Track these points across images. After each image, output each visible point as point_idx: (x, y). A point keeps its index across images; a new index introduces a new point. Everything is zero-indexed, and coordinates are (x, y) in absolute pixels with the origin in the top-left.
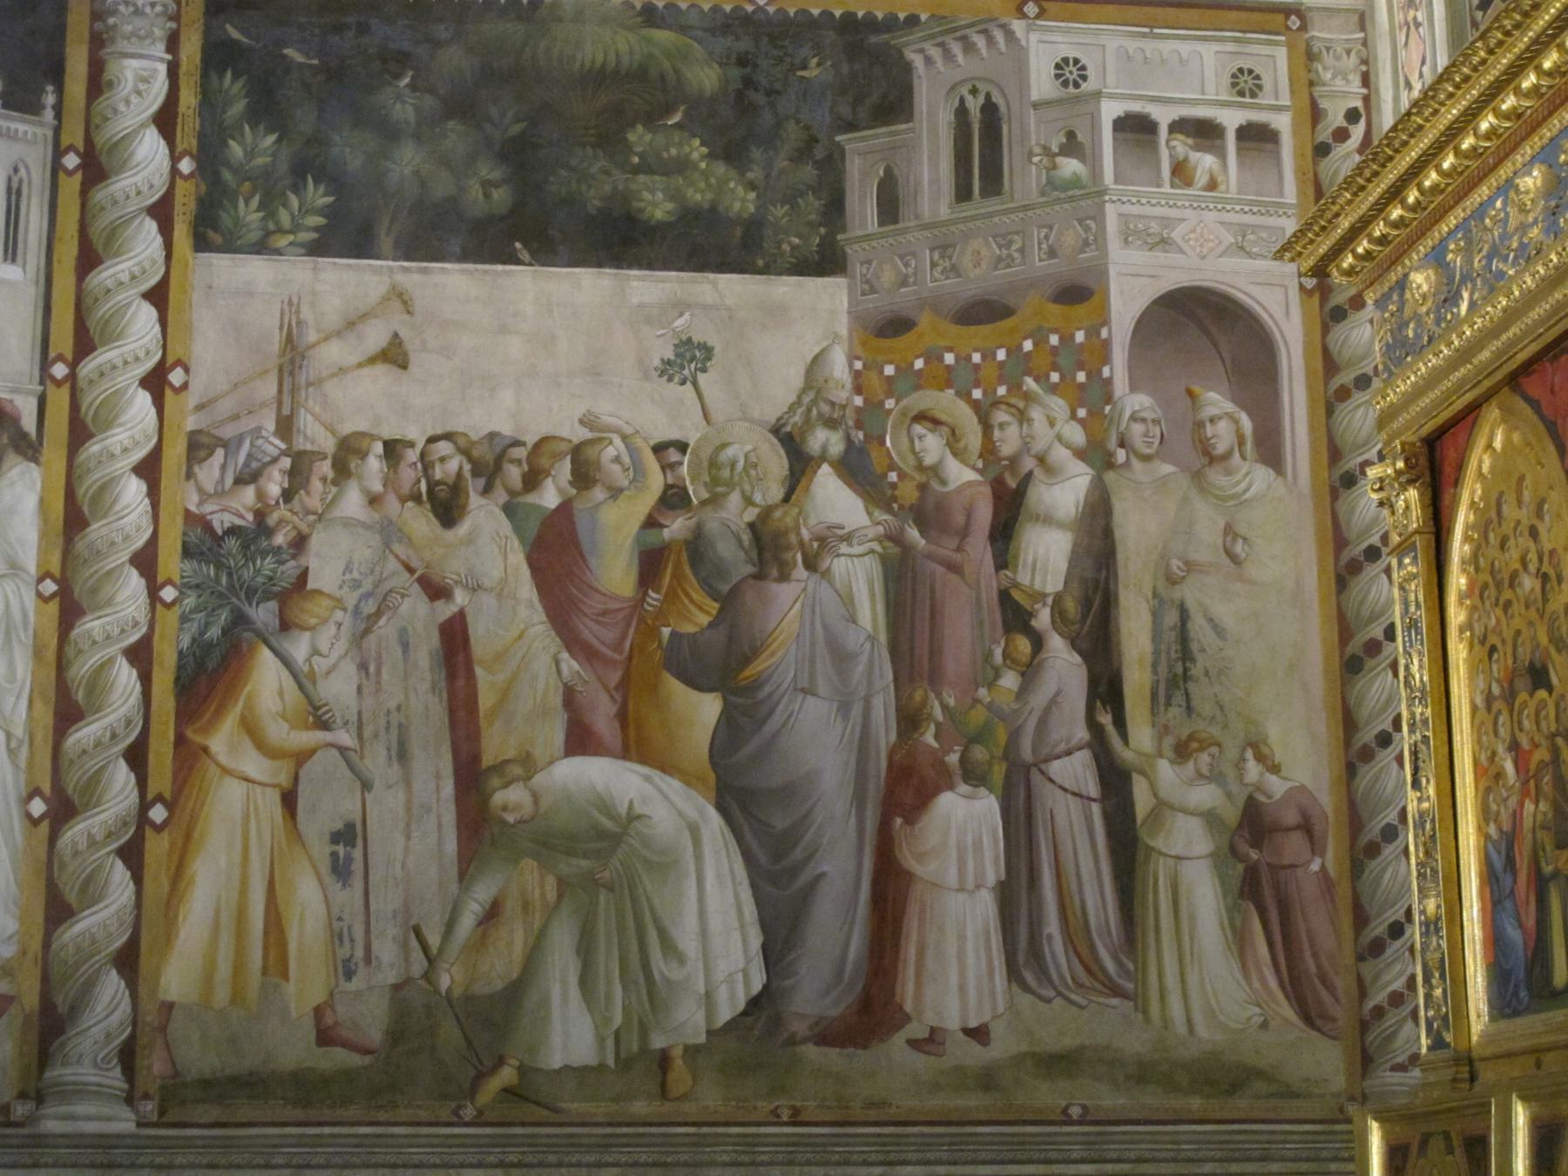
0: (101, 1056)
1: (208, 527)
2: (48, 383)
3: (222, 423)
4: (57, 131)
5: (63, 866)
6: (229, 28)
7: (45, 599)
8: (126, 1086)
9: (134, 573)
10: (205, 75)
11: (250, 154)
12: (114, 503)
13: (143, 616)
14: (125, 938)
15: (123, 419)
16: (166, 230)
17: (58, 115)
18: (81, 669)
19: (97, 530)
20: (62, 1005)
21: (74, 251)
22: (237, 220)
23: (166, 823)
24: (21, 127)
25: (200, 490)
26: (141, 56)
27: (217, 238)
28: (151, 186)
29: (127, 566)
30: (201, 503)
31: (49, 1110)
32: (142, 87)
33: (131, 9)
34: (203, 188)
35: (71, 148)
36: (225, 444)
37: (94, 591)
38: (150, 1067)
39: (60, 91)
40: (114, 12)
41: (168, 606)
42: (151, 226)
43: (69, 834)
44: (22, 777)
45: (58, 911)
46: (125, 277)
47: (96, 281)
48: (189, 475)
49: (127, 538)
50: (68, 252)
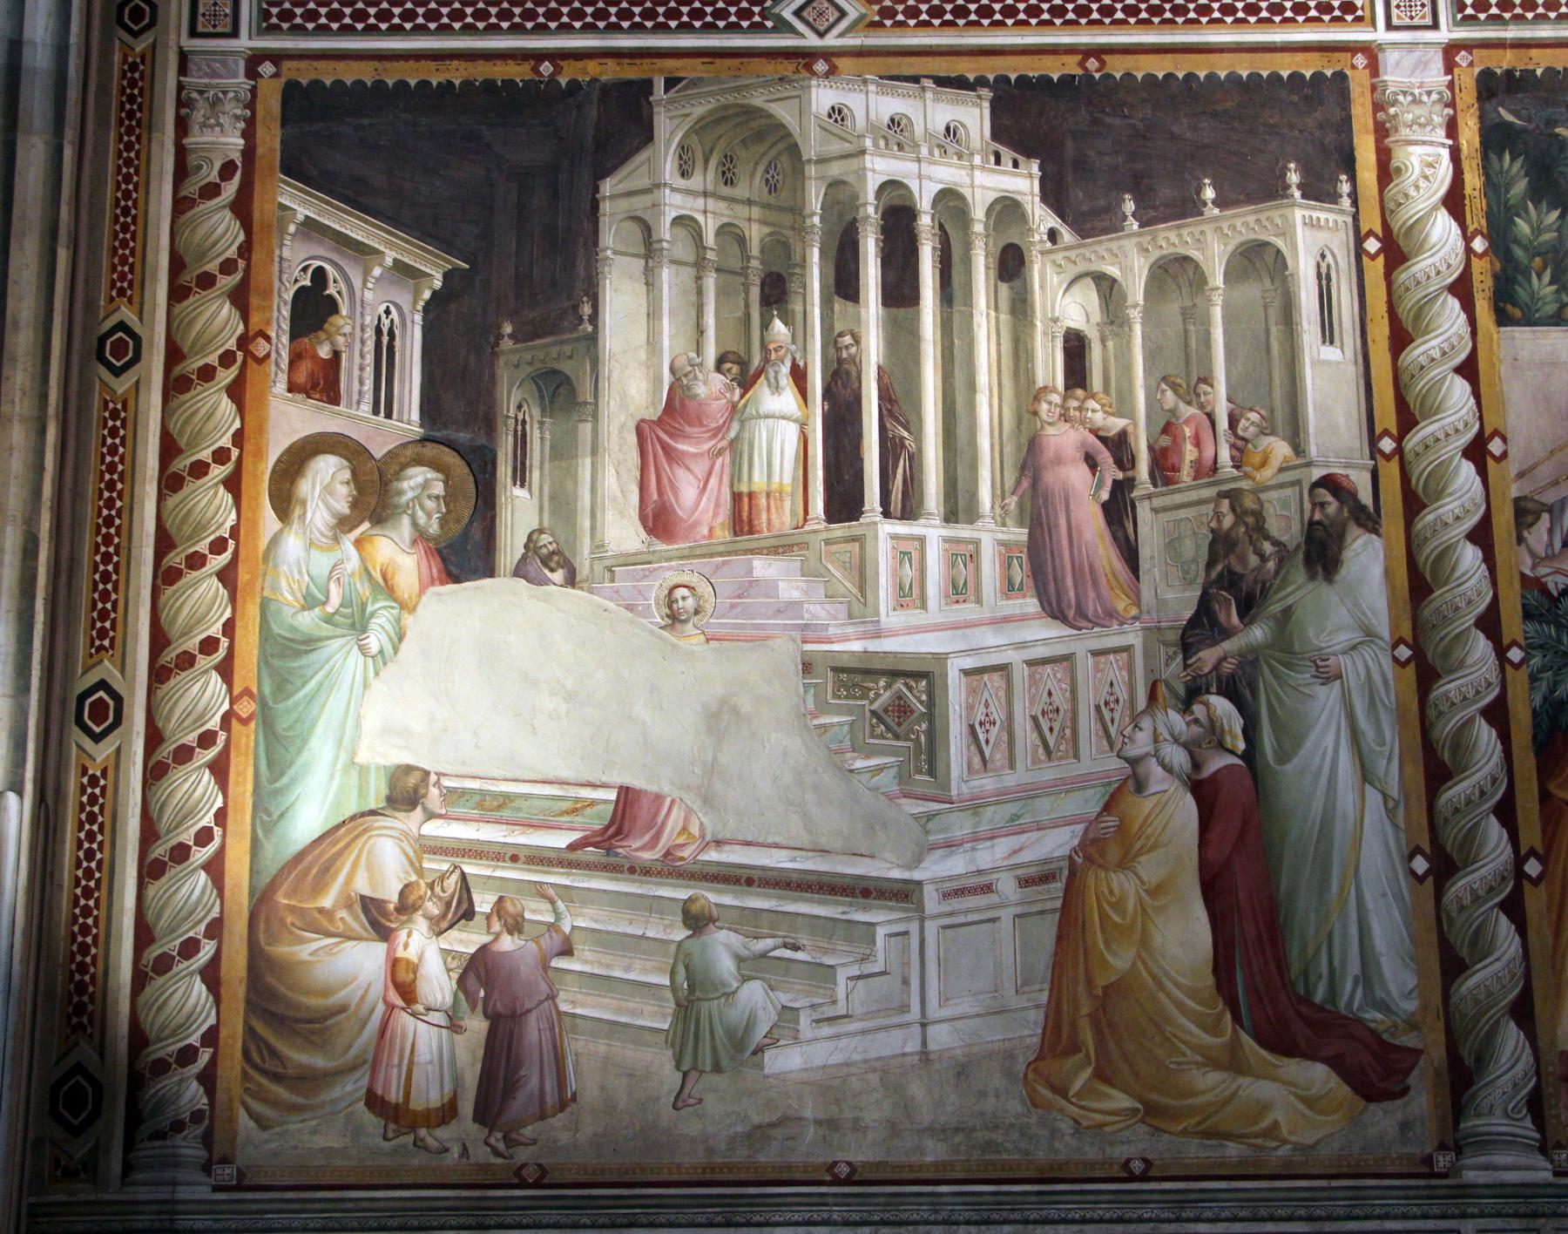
0: (1510, 1107)
1: (1544, 590)
2: (1378, 457)
3: (1543, 489)
4: (1356, 217)
5: (1451, 921)
6: (1501, 109)
7: (1403, 665)
8: (1538, 1136)
9: (1481, 636)
10: (1485, 158)
11: (1537, 230)
12: (1453, 569)
13: (1494, 677)
14: (1517, 991)
15: (1450, 490)
16: (1468, 306)
17: (1355, 203)
18: (1445, 729)
19: (1440, 597)
20: (1468, 1058)
21: (1386, 331)
22: (1532, 294)
23: (1541, 876)
24: (1323, 216)
25: (1532, 554)
26: (1424, 143)
27: (1518, 313)
28: (1449, 266)
29: (1473, 629)
30: (1534, 567)
31: (1468, 1161)
32: (1429, 172)
33: (1409, 98)
34: (1498, 266)
35: (1370, 233)
36: (1550, 510)
37: (1446, 654)
38: (1558, 1117)
39: (1353, 179)
40: (1394, 103)
41: (1517, 666)
42: (1454, 304)
43: (1453, 889)
44: (1403, 835)
45: (1453, 966)
46: (1436, 354)
47: (1409, 359)
48: (1520, 540)
49: (1470, 602)
50: (1380, 331)
